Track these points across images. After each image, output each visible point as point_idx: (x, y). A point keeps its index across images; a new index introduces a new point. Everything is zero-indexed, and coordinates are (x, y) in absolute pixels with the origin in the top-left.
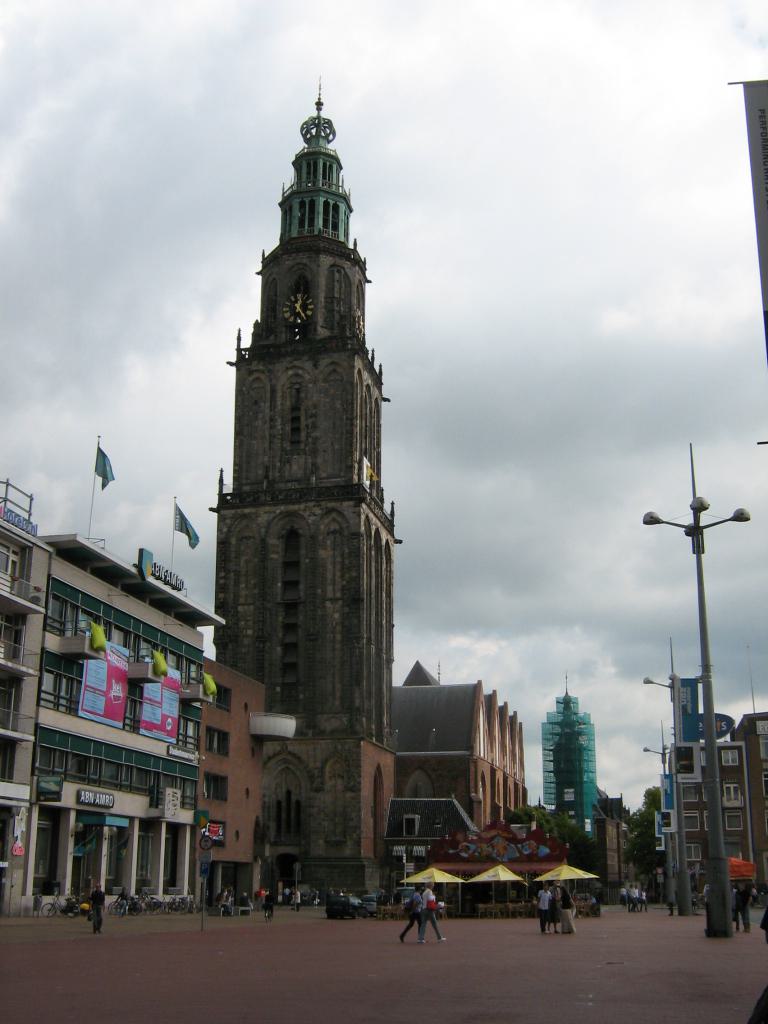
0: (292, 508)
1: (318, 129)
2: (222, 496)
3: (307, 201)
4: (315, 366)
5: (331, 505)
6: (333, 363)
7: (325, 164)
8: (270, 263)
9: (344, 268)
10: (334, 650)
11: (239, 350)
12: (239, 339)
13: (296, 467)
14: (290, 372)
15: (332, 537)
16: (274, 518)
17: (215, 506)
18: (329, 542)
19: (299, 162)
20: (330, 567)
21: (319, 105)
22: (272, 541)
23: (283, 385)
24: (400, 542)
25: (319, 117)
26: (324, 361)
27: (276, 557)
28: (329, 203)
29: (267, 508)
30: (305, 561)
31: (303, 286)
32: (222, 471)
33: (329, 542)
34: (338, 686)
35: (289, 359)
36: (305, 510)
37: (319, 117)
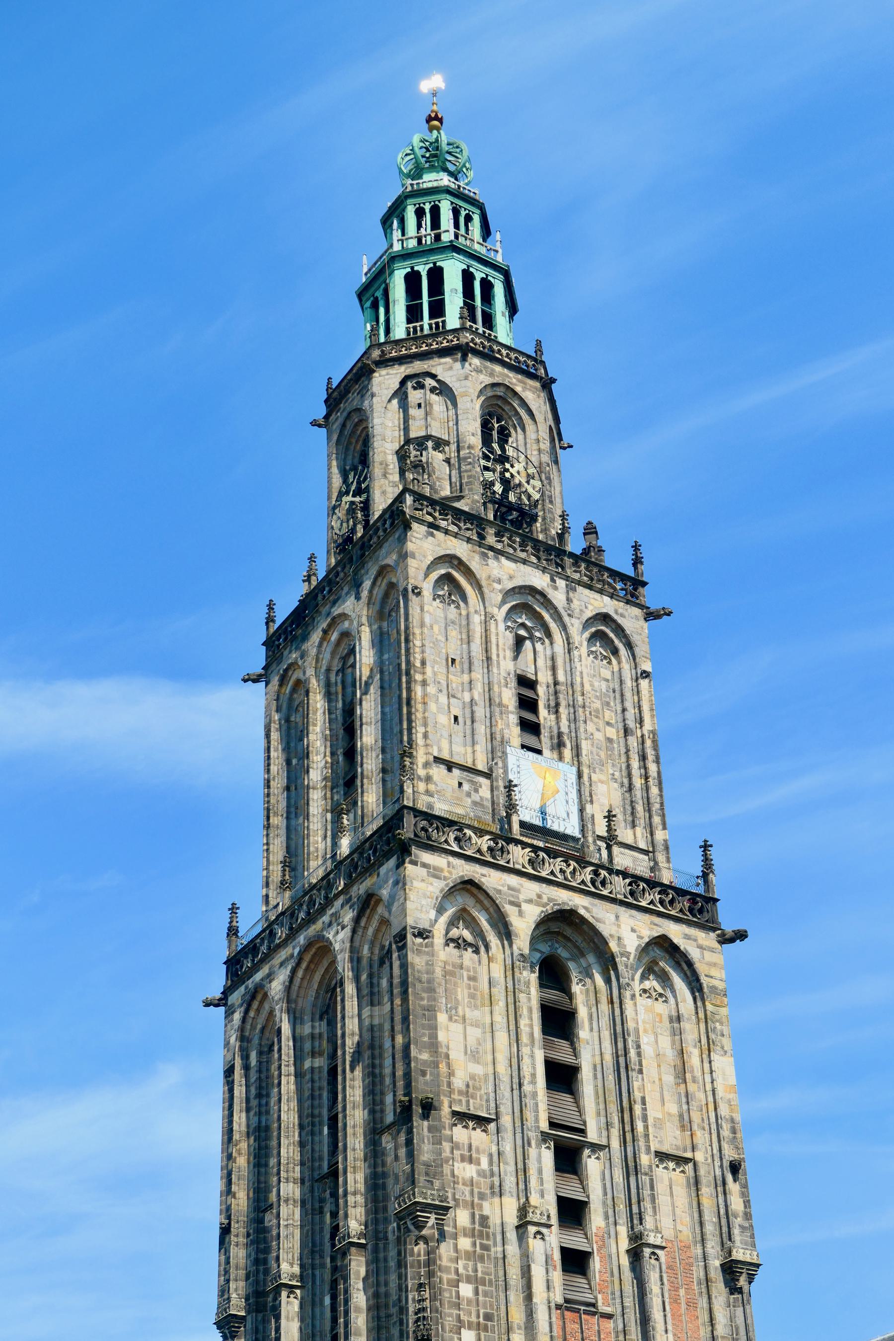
0: (312, 930)
3: (379, 294)
4: (358, 598)
7: (420, 213)
9: (433, 376)
12: (270, 620)
14: (334, 637)
16: (294, 971)
18: (384, 983)
23: (328, 670)
24: (741, 935)
28: (418, 274)
29: (283, 954)
32: (234, 909)
33: (384, 983)
35: (324, 610)
36: (330, 924)
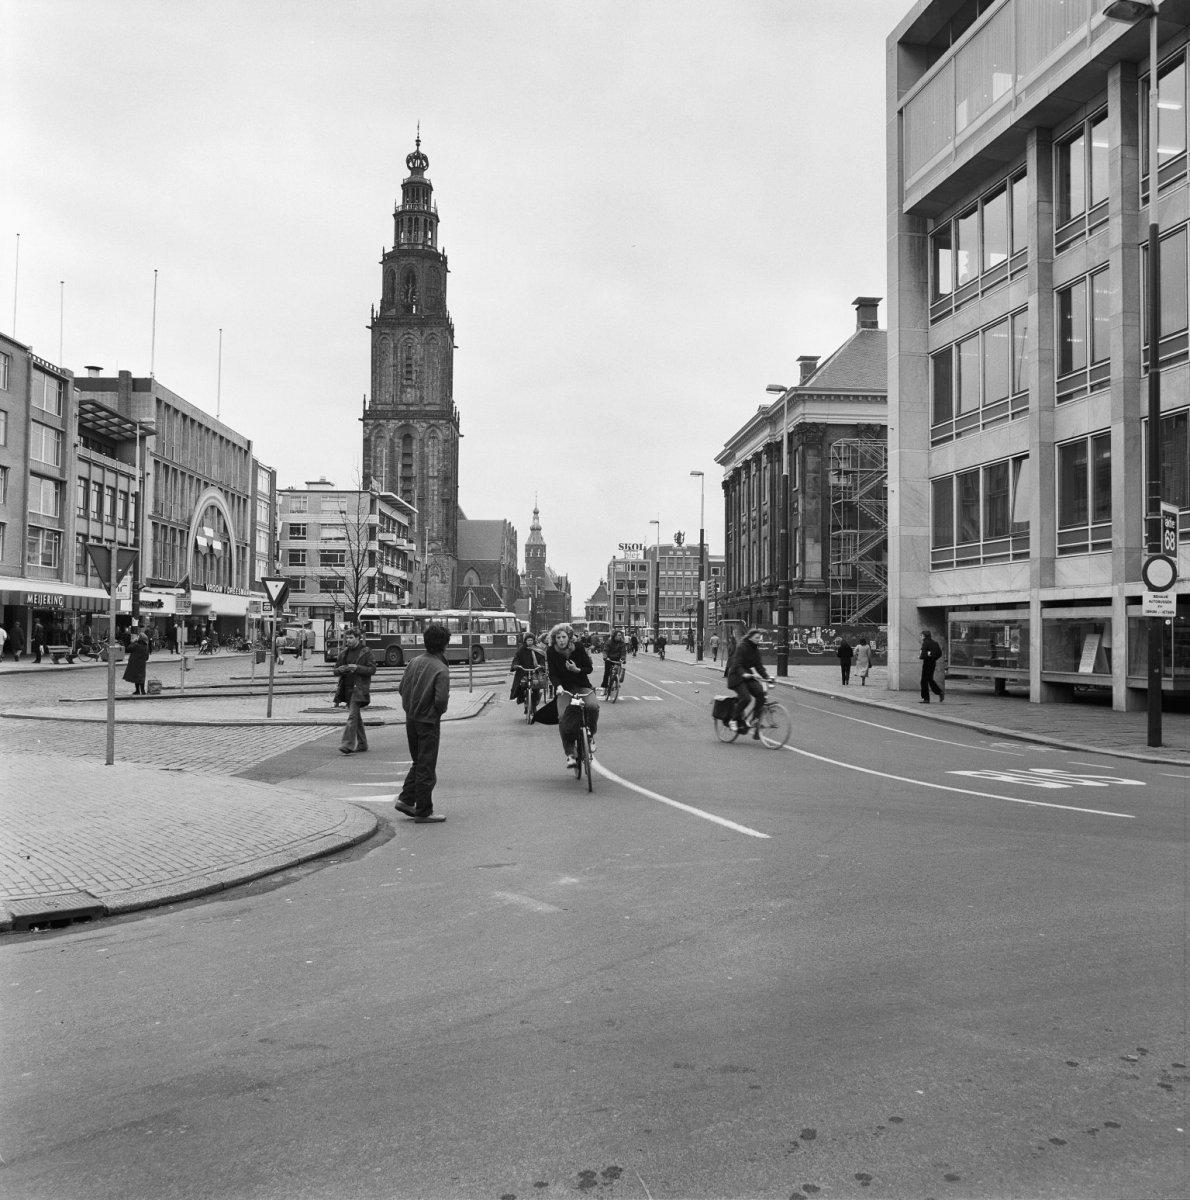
1: (418, 162)
2: (365, 411)
5: (432, 422)
6: (432, 334)
8: (387, 259)
10: (433, 504)
11: (373, 318)
12: (373, 310)
13: (411, 395)
15: (431, 440)
17: (361, 417)
19: (407, 187)
20: (430, 457)
21: (418, 141)
22: (396, 440)
25: (418, 151)
26: (427, 332)
27: (399, 450)
30: (416, 454)
31: (410, 278)
34: (435, 525)
37: (418, 151)
